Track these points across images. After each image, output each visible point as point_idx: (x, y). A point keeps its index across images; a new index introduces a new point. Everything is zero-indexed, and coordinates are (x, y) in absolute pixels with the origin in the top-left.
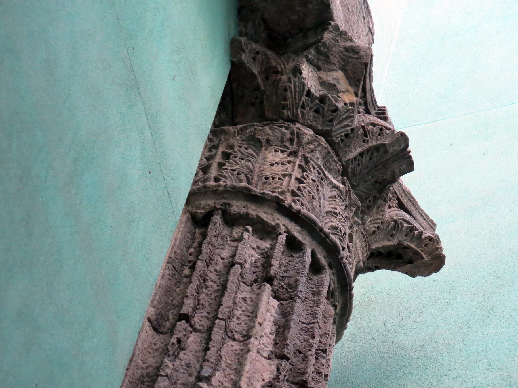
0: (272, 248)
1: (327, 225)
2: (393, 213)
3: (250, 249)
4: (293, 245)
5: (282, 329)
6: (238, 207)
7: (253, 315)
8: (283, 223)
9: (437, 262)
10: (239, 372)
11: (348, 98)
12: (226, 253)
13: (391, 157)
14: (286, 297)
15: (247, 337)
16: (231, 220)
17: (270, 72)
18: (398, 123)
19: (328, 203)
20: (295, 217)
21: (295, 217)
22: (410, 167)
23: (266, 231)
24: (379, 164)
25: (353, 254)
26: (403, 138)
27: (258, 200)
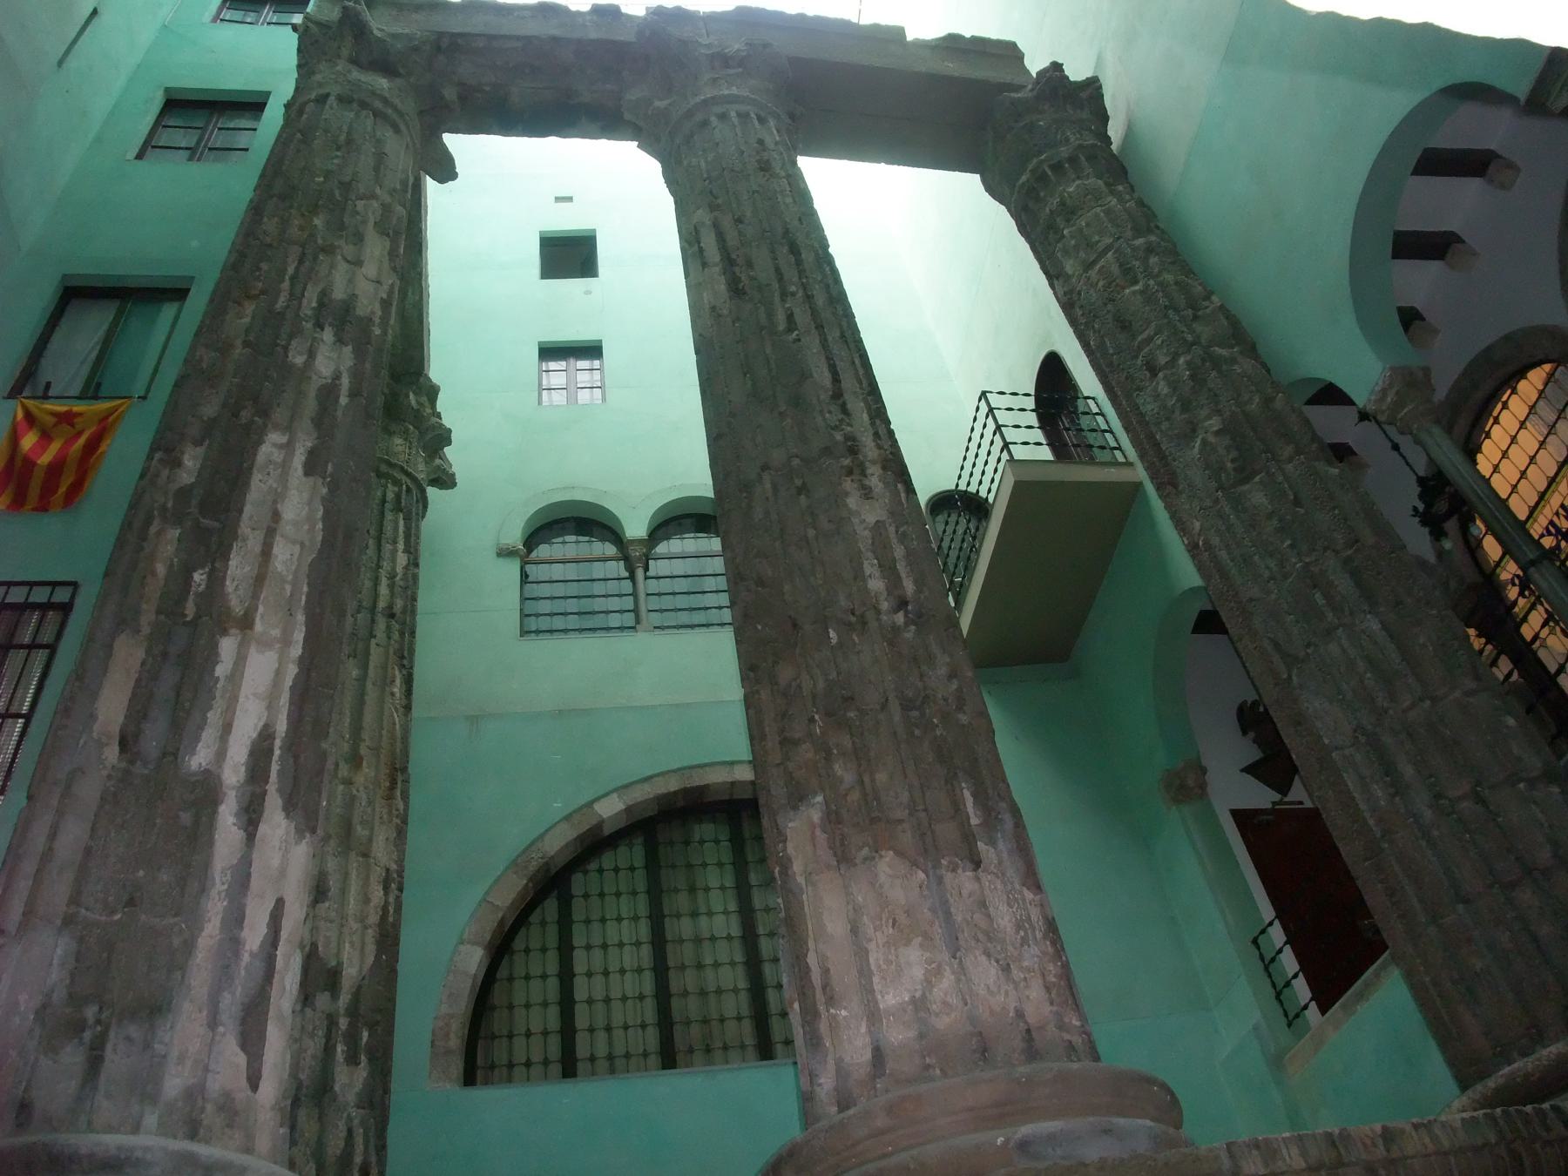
0: (400, 490)
1: (421, 476)
4: (409, 490)
6: (384, 468)
7: (396, 529)
8: (404, 478)
11: (429, 411)
12: (379, 494)
13: (444, 437)
14: (407, 519)
15: (395, 542)
18: (447, 421)
19: (421, 471)
22: (449, 443)
23: (397, 482)
26: (450, 431)
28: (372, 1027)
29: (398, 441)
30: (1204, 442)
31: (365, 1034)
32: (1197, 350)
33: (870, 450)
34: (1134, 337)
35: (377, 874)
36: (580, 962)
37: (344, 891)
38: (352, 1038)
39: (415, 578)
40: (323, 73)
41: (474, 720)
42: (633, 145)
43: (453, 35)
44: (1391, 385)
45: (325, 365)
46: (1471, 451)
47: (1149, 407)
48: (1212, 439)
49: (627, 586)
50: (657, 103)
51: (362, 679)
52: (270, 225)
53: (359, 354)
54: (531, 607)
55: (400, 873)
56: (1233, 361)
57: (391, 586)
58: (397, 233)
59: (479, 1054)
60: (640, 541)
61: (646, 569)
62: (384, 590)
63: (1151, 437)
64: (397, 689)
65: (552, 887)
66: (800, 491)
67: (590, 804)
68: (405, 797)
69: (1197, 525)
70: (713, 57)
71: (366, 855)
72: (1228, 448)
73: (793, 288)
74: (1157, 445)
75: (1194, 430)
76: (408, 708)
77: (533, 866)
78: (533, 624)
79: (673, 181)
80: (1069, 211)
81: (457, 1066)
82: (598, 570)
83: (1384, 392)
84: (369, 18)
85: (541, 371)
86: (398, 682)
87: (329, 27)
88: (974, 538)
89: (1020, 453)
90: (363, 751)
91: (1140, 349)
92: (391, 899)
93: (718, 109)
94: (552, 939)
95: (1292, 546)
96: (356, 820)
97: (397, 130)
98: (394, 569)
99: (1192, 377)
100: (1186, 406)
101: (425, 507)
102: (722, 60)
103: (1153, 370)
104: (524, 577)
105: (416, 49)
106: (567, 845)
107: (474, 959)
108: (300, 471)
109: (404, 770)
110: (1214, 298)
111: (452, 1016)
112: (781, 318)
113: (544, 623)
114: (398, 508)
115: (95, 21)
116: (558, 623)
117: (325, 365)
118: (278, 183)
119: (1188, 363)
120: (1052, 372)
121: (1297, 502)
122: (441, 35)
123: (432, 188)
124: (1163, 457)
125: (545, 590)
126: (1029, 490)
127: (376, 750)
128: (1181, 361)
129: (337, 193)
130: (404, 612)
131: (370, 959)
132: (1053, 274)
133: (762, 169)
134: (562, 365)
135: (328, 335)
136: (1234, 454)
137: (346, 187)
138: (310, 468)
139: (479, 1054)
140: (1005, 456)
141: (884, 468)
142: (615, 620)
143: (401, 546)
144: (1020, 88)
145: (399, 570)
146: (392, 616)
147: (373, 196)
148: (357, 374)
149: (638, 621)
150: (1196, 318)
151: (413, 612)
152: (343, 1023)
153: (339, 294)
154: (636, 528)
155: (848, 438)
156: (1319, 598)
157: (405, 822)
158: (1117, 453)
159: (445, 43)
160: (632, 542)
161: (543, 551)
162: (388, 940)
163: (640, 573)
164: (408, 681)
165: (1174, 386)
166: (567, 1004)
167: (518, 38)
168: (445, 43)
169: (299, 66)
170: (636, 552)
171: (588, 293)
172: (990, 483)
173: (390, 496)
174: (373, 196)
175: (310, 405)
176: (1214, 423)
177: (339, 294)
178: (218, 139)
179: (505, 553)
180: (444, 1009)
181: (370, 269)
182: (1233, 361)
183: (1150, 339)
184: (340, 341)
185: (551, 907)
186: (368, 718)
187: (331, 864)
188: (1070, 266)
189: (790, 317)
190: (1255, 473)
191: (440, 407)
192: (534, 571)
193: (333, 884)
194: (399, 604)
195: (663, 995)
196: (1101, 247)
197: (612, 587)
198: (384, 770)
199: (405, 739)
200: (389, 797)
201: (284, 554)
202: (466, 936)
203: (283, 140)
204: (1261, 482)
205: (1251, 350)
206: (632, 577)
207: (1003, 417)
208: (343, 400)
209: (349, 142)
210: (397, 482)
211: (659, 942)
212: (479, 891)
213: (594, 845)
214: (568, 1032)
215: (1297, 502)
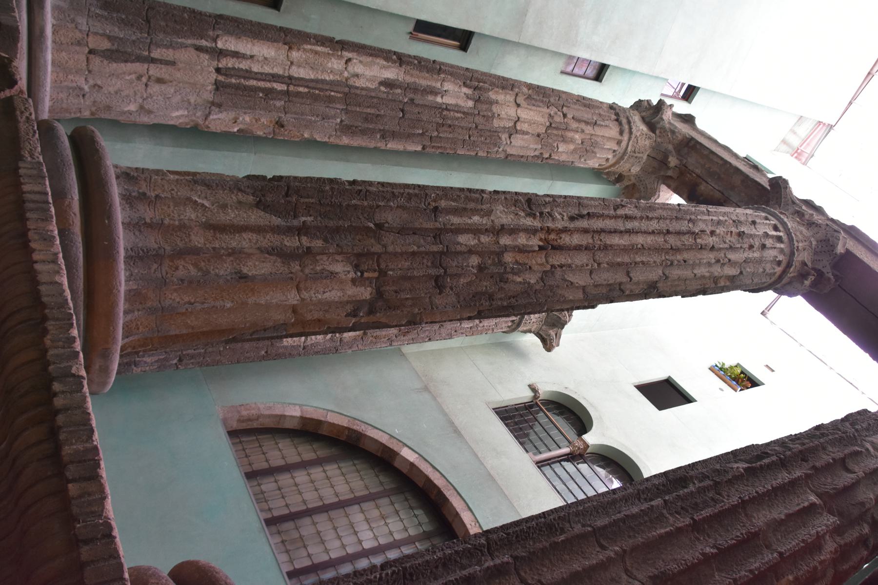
2: (552, 333)
41: (426, 389)
43: (697, 142)
45: (448, 86)
59: (246, 433)
70: (798, 212)
77: (355, 427)
81: (235, 425)
97: (621, 133)
105: (673, 132)
106: (376, 441)
111: (259, 409)
117: (448, 86)
122: (692, 139)
139: (246, 433)
153: (492, 95)
159: (693, 142)
166: (288, 468)
167: (722, 159)
168: (693, 142)
171: (721, 390)
180: (262, 407)
181: (523, 114)
195: (309, 513)
201: (336, 64)
211: (341, 505)
214: (271, 471)
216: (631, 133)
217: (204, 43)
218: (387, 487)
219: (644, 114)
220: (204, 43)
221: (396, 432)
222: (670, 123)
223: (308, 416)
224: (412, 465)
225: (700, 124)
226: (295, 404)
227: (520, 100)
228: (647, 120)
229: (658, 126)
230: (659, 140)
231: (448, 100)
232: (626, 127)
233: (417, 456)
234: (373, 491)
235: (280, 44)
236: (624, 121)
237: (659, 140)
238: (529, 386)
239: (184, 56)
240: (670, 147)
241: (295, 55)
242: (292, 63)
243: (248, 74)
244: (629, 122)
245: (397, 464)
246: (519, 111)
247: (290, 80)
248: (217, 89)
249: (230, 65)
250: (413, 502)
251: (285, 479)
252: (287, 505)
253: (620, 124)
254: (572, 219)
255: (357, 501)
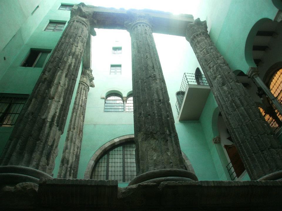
1: (88, 84)
3: (83, 86)
4: (86, 86)
5: (85, 94)
6: (82, 83)
7: (83, 93)
9: (94, 87)
10: (83, 98)
12: (81, 87)
13: (93, 79)
14: (86, 91)
16: (81, 84)
17: (85, 71)
19: (88, 83)
20: (86, 84)
21: (86, 84)
23: (84, 85)
24: (92, 79)
25: (89, 86)
27: (84, 82)
28: (74, 170)
29: (85, 78)
30: (218, 79)
31: (73, 171)
32: (218, 65)
33: (158, 77)
34: (207, 62)
35: (76, 147)
36: (110, 165)
37: (70, 149)
38: (70, 171)
39: (86, 101)
40: (75, 17)
41: (95, 125)
42: (126, 31)
44: (251, 70)
46: (268, 85)
47: (209, 74)
48: (219, 79)
49: (123, 105)
50: (129, 24)
51: (76, 116)
52: (63, 40)
53: (76, 60)
54: (106, 107)
55: (80, 147)
56: (224, 66)
57: (82, 101)
58: (84, 43)
60: (125, 97)
61: (126, 102)
62: (81, 102)
63: (209, 79)
64: (82, 118)
65: (106, 152)
66: (145, 82)
67: (113, 139)
68: (82, 135)
69: (216, 93)
71: (74, 143)
72: (221, 80)
73: (148, 52)
74: (210, 80)
75: (216, 78)
76: (83, 121)
77: (103, 149)
78: (106, 110)
79: (131, 36)
80: (198, 42)
82: (118, 102)
83: (249, 72)
84: (82, 8)
85: (111, 69)
86: (82, 117)
87: (76, 10)
88: (183, 98)
89: (190, 83)
90: (75, 127)
91: (208, 64)
92: (79, 151)
93: (140, 24)
94: (106, 161)
95: (230, 96)
96: (73, 138)
98: (82, 99)
99: (216, 69)
100: (215, 73)
101: (89, 89)
102: (141, 17)
103: (210, 68)
104: (105, 103)
105: (90, 14)
107: (92, 163)
108: (64, 77)
109: (82, 131)
110: (222, 56)
112: (145, 56)
113: (108, 110)
114: (84, 89)
115: (38, 8)
116: (110, 110)
117: (69, 61)
118: (65, 35)
119: (216, 67)
120: (198, 70)
121: (232, 89)
122: (94, 12)
123: (92, 37)
124: (211, 82)
125: (109, 105)
126: (192, 90)
127: (77, 127)
128: (215, 66)
129: (75, 36)
130: (84, 106)
131: (74, 160)
132: (196, 53)
133: (145, 34)
134: (114, 68)
135: (71, 57)
136: (222, 81)
137: (76, 35)
138: (66, 76)
140: (188, 83)
141: (160, 80)
142: (120, 110)
143: (84, 95)
144: (192, 22)
145: (83, 99)
146: (82, 106)
147: (81, 36)
148: (75, 63)
149: (124, 110)
150: (218, 59)
151: (85, 106)
152: (69, 169)
153: (73, 51)
154: (125, 95)
155: (154, 75)
156: (234, 104)
157: (82, 139)
158: (207, 84)
159: (95, 13)
160: (124, 97)
161: (109, 98)
162: (78, 157)
163: (125, 102)
164: (84, 117)
165: (213, 70)
166: (107, 171)
168: (95, 13)
169: (71, 16)
170: (124, 99)
172: (185, 89)
173: (83, 87)
174: (81, 36)
175: (67, 67)
176: (219, 76)
177: (73, 51)
178: (58, 28)
179: (103, 98)
181: (79, 48)
182: (224, 66)
183: (210, 63)
184: (73, 58)
185: (106, 156)
186: (76, 122)
187: (69, 144)
188: (198, 51)
189: (147, 56)
190: (225, 84)
191: (92, 74)
192: (106, 101)
193: (69, 147)
194: (83, 104)
195: (124, 171)
196: (203, 48)
197: (120, 105)
198: (78, 131)
199: (82, 126)
200: (79, 135)
201: (60, 88)
202: (91, 159)
203: (67, 28)
204: (226, 86)
205: (227, 65)
206: (124, 103)
207: (188, 77)
208: (72, 67)
209: (77, 28)
210: (84, 85)
212: (93, 152)
213: (113, 146)
215: (232, 89)
216: (87, 24)
217: (48, 124)
218: (121, 149)
219: (78, 14)
220: (48, 124)
221: (108, 140)
222: (87, 12)
223: (95, 159)
224: (120, 141)
225: (86, 4)
226: (89, 161)
227: (76, 44)
228: (81, 15)
229: (86, 16)
230: (89, 19)
231: (73, 64)
232: (85, 24)
233: (118, 138)
234: (122, 153)
235: (50, 101)
236: (83, 22)
237: (89, 19)
238: (101, 99)
239: (51, 135)
240: (92, 19)
241: (56, 98)
242: (60, 102)
243: (59, 117)
244: (84, 22)
245: (116, 144)
246: (78, 47)
247: (62, 105)
248: (61, 130)
249: (55, 121)
250: (128, 146)
251: (110, 173)
252: (120, 176)
253: (84, 24)
254: (154, 70)
255: (124, 158)
